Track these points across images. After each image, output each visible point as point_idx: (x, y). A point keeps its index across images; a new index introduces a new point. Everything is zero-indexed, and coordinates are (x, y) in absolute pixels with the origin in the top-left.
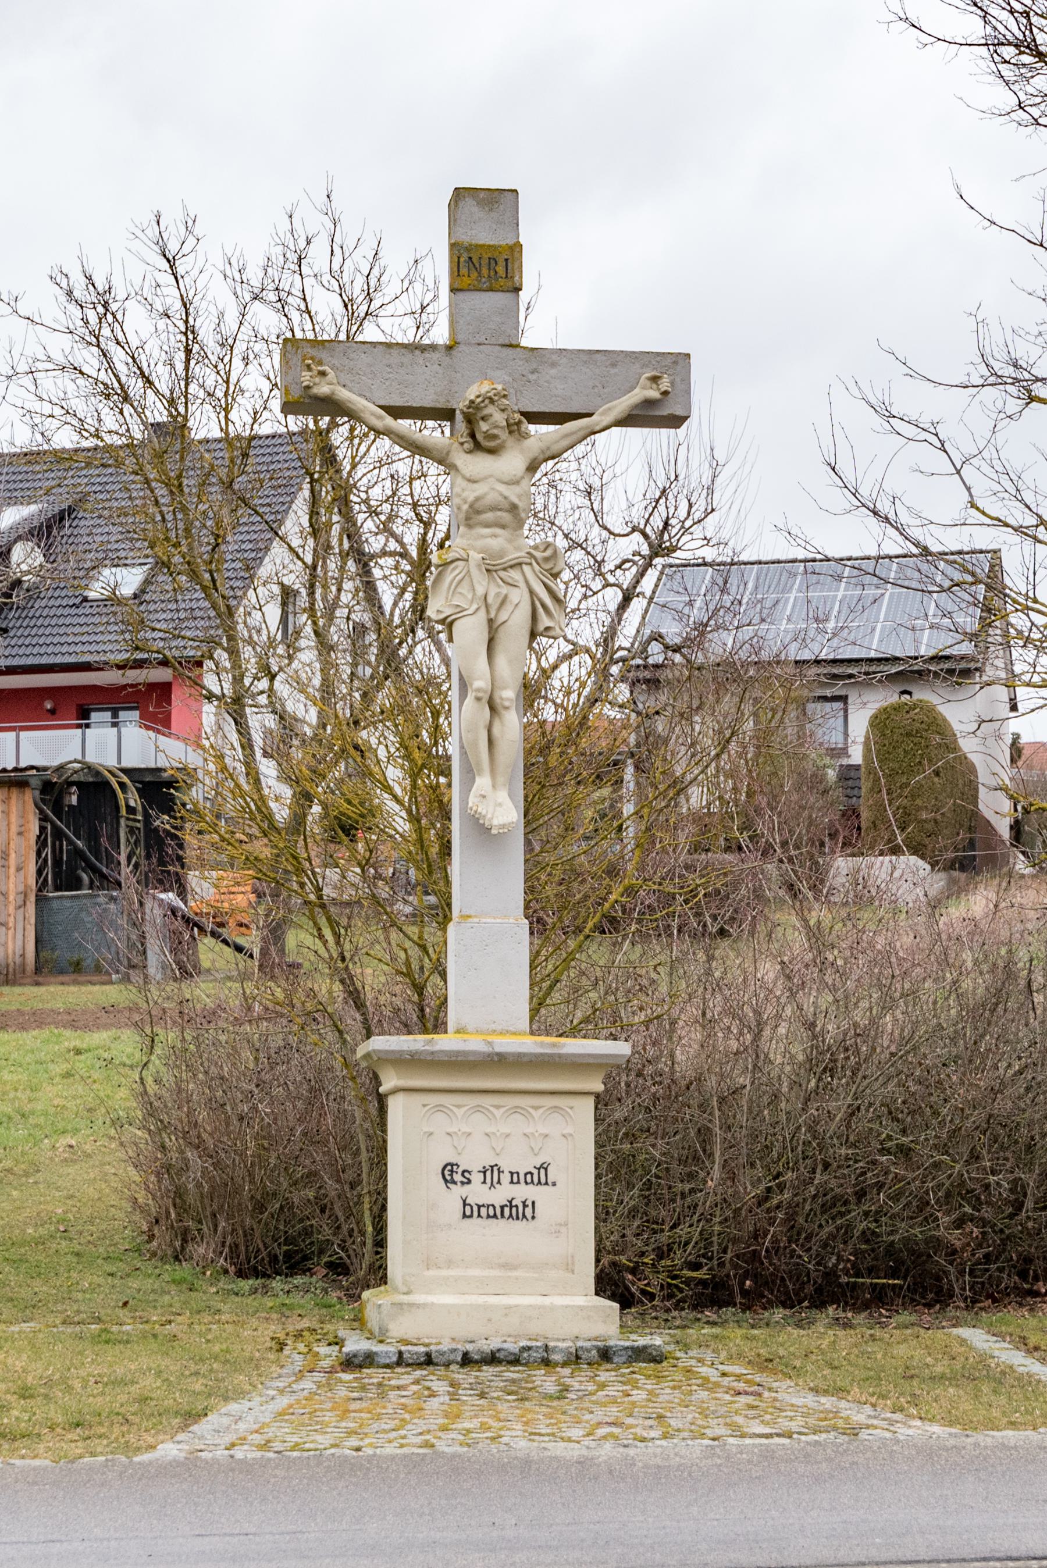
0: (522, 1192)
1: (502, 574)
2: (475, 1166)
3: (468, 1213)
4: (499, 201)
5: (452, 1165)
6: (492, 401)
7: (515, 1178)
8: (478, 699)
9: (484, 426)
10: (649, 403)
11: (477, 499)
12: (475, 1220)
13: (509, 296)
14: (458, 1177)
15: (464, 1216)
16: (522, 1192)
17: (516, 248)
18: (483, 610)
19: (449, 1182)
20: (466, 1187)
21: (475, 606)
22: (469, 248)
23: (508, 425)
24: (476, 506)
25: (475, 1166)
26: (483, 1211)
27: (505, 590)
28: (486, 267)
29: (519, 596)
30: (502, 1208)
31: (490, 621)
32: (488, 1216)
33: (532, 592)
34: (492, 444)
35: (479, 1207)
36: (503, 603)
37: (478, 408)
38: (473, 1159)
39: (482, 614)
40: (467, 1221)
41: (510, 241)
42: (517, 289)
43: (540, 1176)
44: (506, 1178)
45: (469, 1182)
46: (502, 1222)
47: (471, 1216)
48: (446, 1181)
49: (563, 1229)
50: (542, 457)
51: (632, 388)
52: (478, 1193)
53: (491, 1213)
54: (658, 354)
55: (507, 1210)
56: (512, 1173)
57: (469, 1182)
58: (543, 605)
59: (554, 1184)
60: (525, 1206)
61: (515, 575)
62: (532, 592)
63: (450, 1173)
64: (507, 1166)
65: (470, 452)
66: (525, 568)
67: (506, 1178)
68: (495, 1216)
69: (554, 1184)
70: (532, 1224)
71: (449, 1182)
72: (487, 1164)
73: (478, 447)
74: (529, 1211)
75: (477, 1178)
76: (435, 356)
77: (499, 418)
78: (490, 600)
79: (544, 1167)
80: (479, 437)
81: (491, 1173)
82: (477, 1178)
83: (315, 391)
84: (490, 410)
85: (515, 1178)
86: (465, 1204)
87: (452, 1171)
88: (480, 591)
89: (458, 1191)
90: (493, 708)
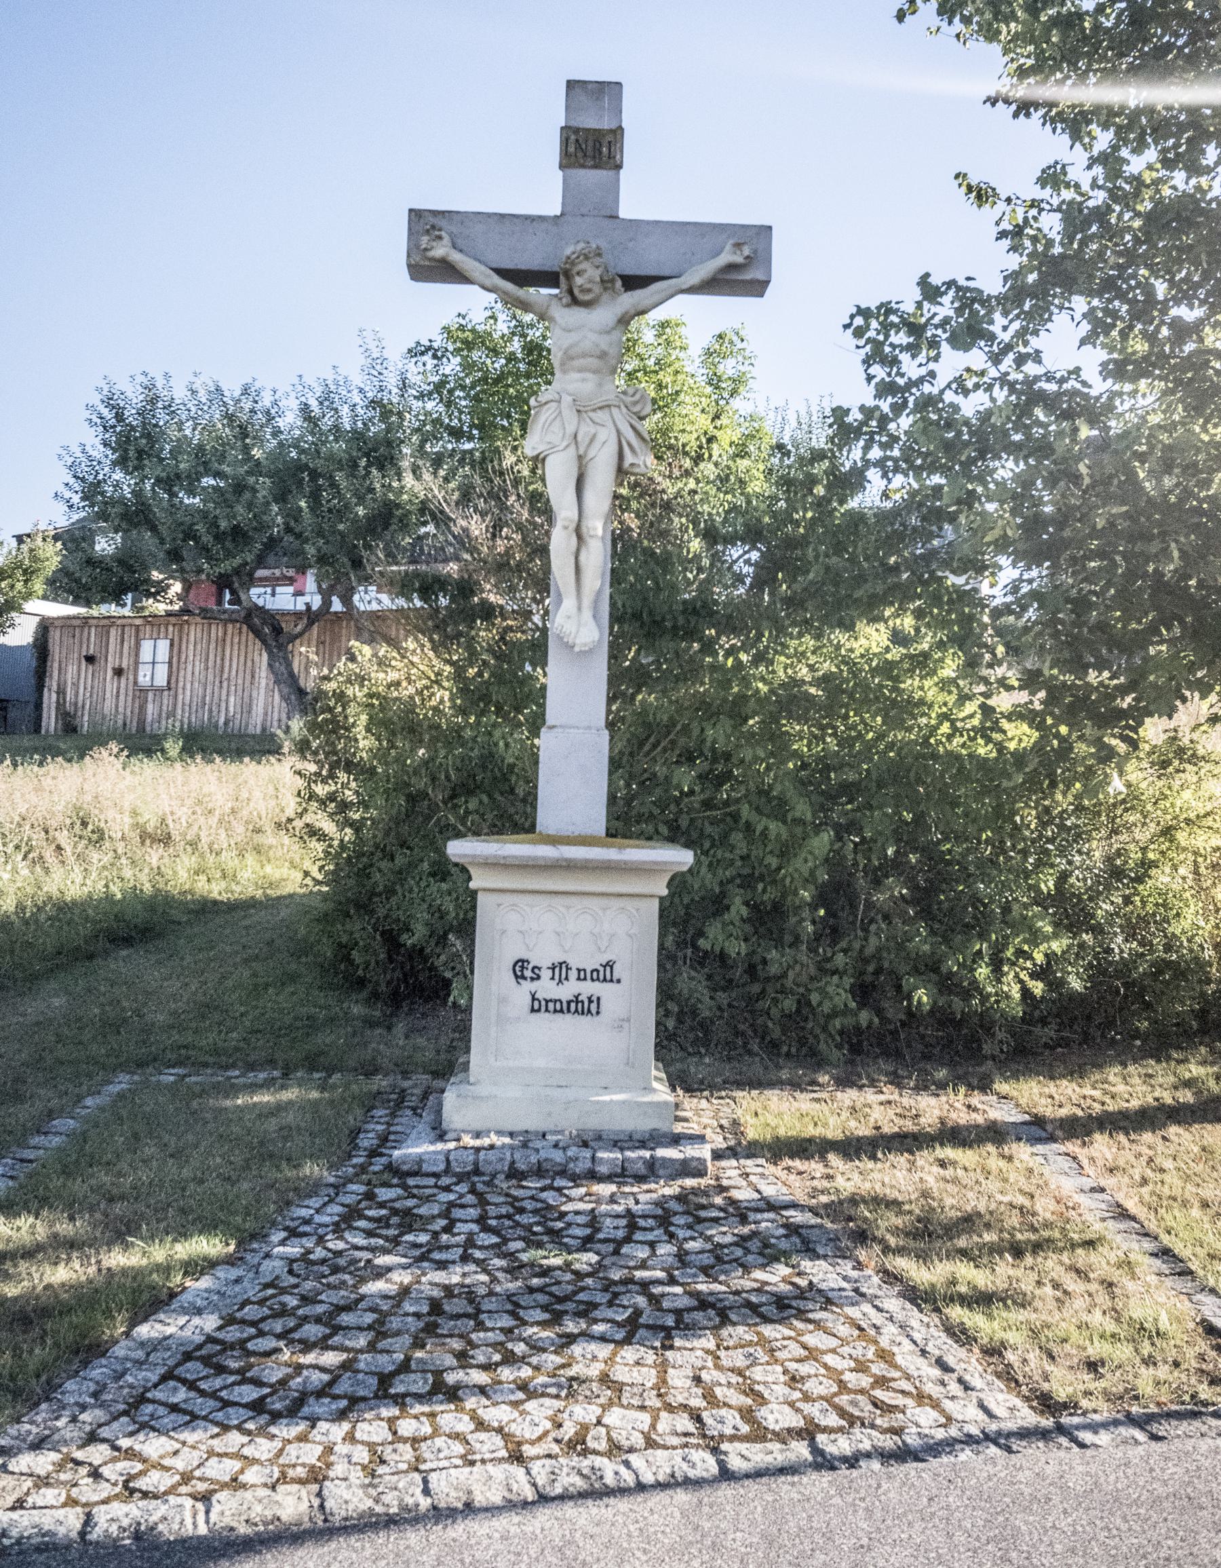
0: (588, 988)
1: (591, 414)
2: (545, 963)
3: (536, 1007)
4: (606, 92)
5: (523, 961)
6: (587, 258)
7: (582, 975)
8: (566, 528)
9: (579, 281)
10: (731, 267)
11: (571, 346)
12: (543, 1015)
13: (611, 173)
14: (528, 973)
15: (533, 1010)
16: (588, 988)
17: (618, 132)
18: (573, 447)
19: (520, 977)
20: (536, 983)
21: (565, 444)
22: (577, 131)
23: (602, 281)
24: (571, 352)
25: (545, 963)
26: (551, 1006)
27: (592, 429)
28: (591, 147)
29: (607, 435)
30: (569, 1003)
31: (580, 458)
32: (555, 1011)
33: (618, 432)
34: (587, 297)
35: (547, 1001)
36: (592, 441)
37: (573, 264)
38: (543, 957)
39: (572, 450)
40: (535, 1015)
41: (613, 126)
42: (619, 167)
43: (605, 973)
44: (573, 974)
45: (539, 977)
46: (568, 1017)
47: (539, 1010)
48: (517, 977)
49: (626, 1025)
50: (633, 312)
51: (718, 254)
52: (547, 988)
53: (558, 1007)
54: (743, 226)
55: (573, 1005)
56: (579, 970)
57: (539, 977)
58: (629, 445)
59: (619, 981)
60: (590, 1001)
61: (601, 416)
62: (618, 432)
63: (521, 970)
64: (574, 963)
65: (568, 306)
66: (615, 411)
67: (573, 974)
68: (561, 1011)
69: (619, 981)
70: (596, 1019)
71: (520, 977)
72: (557, 960)
73: (575, 302)
74: (594, 1007)
75: (546, 974)
76: (544, 226)
77: (595, 274)
78: (579, 438)
79: (609, 965)
80: (576, 291)
81: (560, 970)
82: (546, 974)
83: (431, 254)
84: (584, 265)
85: (582, 975)
86: (534, 999)
87: (522, 967)
88: (570, 429)
89: (528, 986)
90: (580, 537)
